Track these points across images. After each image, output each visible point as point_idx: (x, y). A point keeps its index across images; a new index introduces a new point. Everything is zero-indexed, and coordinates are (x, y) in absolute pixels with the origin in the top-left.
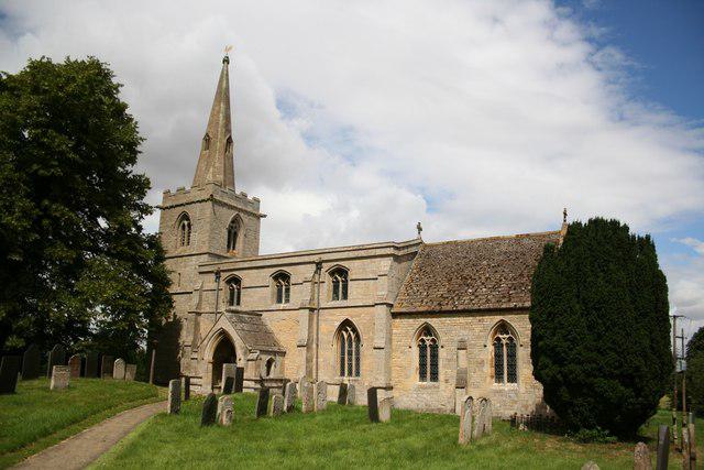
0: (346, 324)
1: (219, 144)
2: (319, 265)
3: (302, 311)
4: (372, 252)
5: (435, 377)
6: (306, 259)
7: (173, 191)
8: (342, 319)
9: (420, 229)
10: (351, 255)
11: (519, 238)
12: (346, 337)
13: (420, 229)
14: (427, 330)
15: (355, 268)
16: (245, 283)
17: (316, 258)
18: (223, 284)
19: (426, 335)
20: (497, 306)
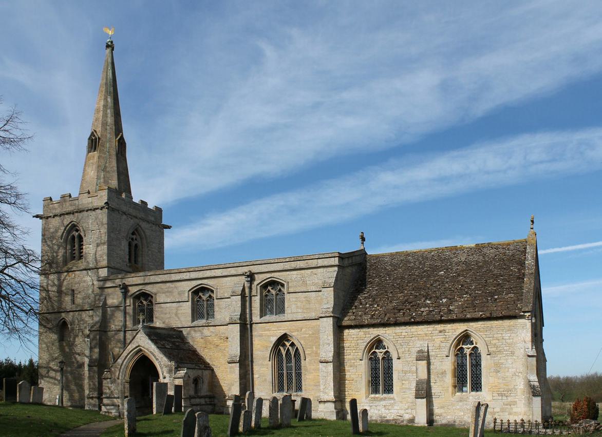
0: (284, 338)
1: (111, 144)
2: (251, 277)
3: (231, 326)
4: (313, 263)
5: (389, 389)
6: (233, 271)
7: (57, 198)
8: (280, 333)
9: (363, 239)
10: (288, 266)
11: (479, 248)
12: (284, 353)
13: (363, 239)
14: (378, 343)
15: (291, 279)
16: (160, 298)
17: (246, 269)
18: (129, 301)
19: (377, 348)
20: (461, 316)
